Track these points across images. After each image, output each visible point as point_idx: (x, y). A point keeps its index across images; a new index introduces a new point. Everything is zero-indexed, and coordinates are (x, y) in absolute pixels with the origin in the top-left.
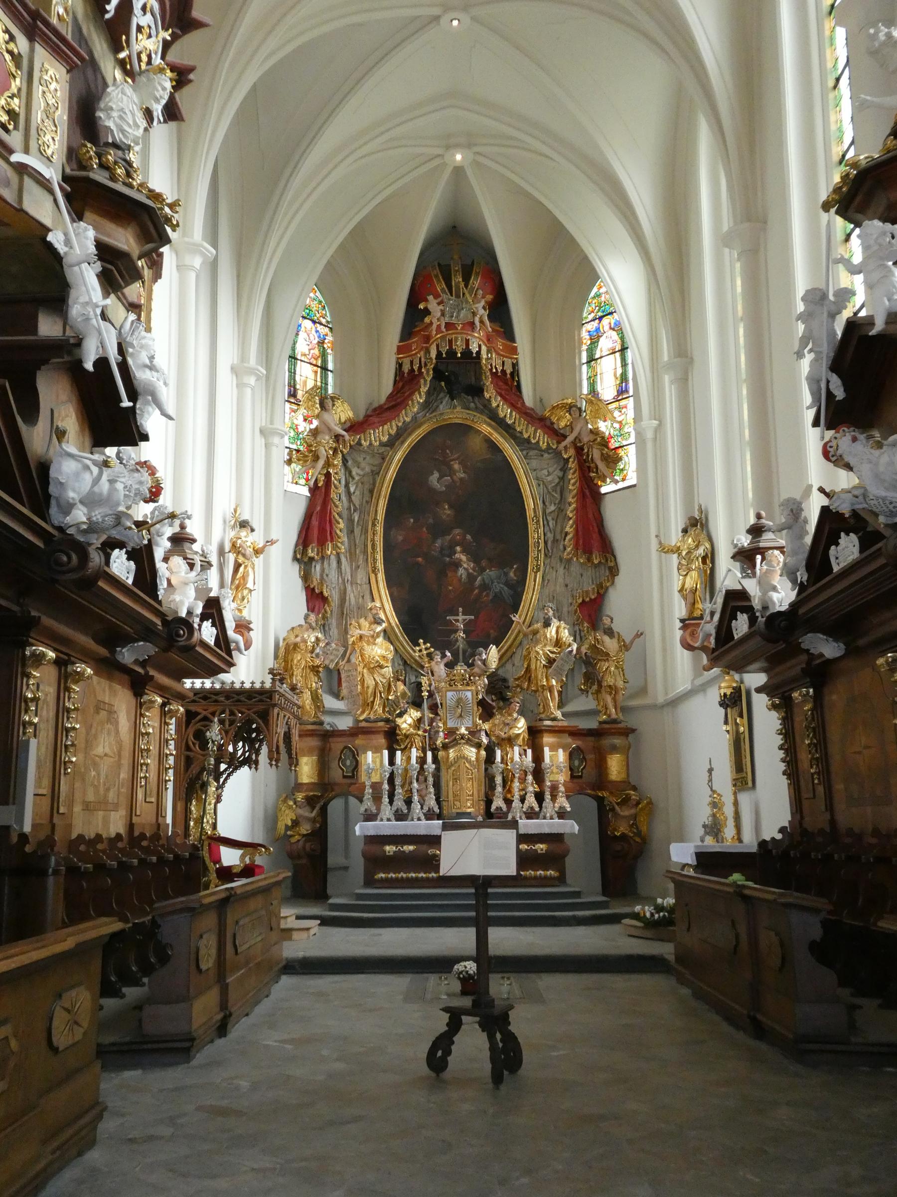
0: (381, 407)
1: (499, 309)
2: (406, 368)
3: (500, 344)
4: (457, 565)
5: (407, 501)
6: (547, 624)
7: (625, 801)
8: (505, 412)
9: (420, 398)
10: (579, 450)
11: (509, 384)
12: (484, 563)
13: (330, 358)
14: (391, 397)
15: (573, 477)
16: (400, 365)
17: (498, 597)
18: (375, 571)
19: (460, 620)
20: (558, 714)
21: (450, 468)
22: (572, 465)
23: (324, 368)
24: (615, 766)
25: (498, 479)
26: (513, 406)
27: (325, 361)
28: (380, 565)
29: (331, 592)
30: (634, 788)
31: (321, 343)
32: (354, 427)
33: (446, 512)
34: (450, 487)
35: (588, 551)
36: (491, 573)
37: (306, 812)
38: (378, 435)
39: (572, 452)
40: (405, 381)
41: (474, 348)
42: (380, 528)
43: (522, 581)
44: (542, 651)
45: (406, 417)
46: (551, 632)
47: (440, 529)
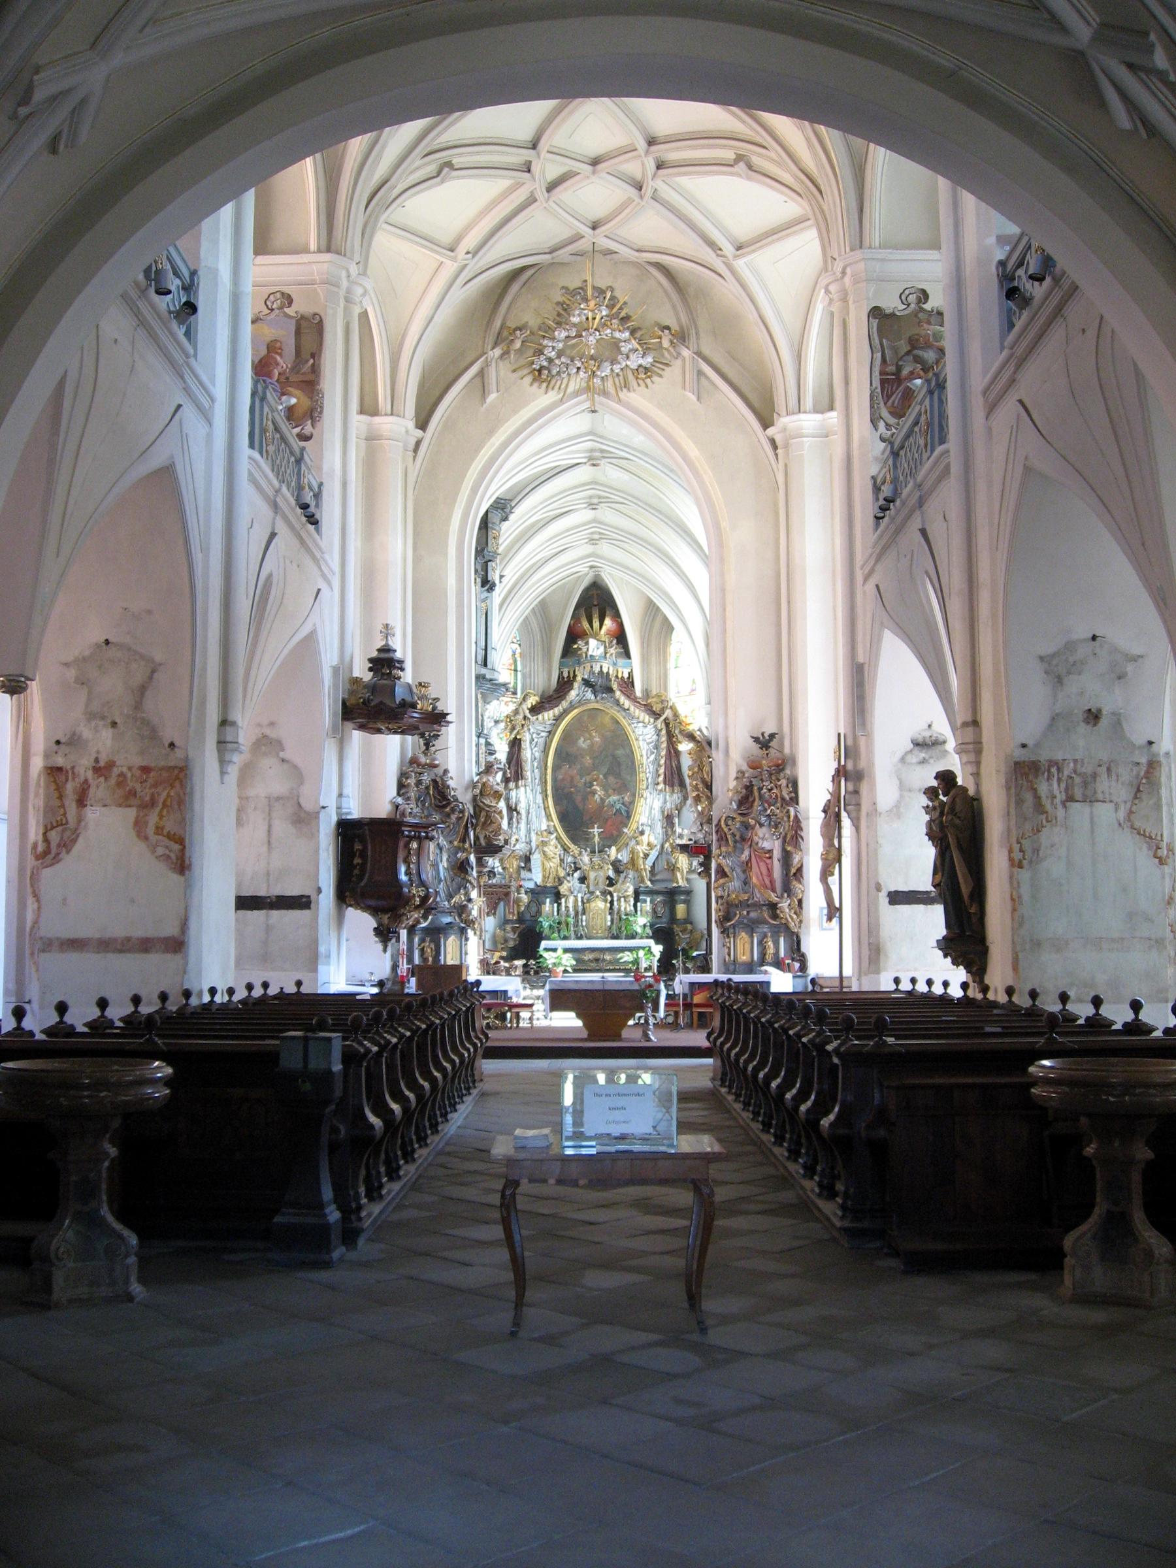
0: (550, 697)
1: (620, 638)
2: (566, 675)
3: (622, 661)
4: (594, 793)
5: (565, 756)
6: (642, 833)
7: (684, 931)
8: (623, 700)
9: (573, 694)
10: (667, 725)
11: (628, 684)
12: (610, 791)
13: (519, 664)
14: (556, 690)
15: (664, 739)
16: (561, 674)
17: (619, 811)
18: (546, 796)
19: (596, 831)
20: (649, 883)
21: (591, 735)
22: (664, 732)
23: (516, 670)
24: (681, 909)
25: (619, 740)
26: (628, 697)
27: (516, 666)
28: (549, 792)
29: (522, 807)
30: (691, 923)
31: (514, 653)
32: (535, 710)
33: (588, 760)
34: (591, 746)
35: (672, 786)
36: (614, 798)
37: (511, 935)
38: (548, 716)
39: (663, 726)
40: (564, 685)
41: (605, 670)
42: (549, 771)
43: (632, 802)
44: (642, 849)
45: (564, 704)
46: (645, 839)
47: (584, 772)
